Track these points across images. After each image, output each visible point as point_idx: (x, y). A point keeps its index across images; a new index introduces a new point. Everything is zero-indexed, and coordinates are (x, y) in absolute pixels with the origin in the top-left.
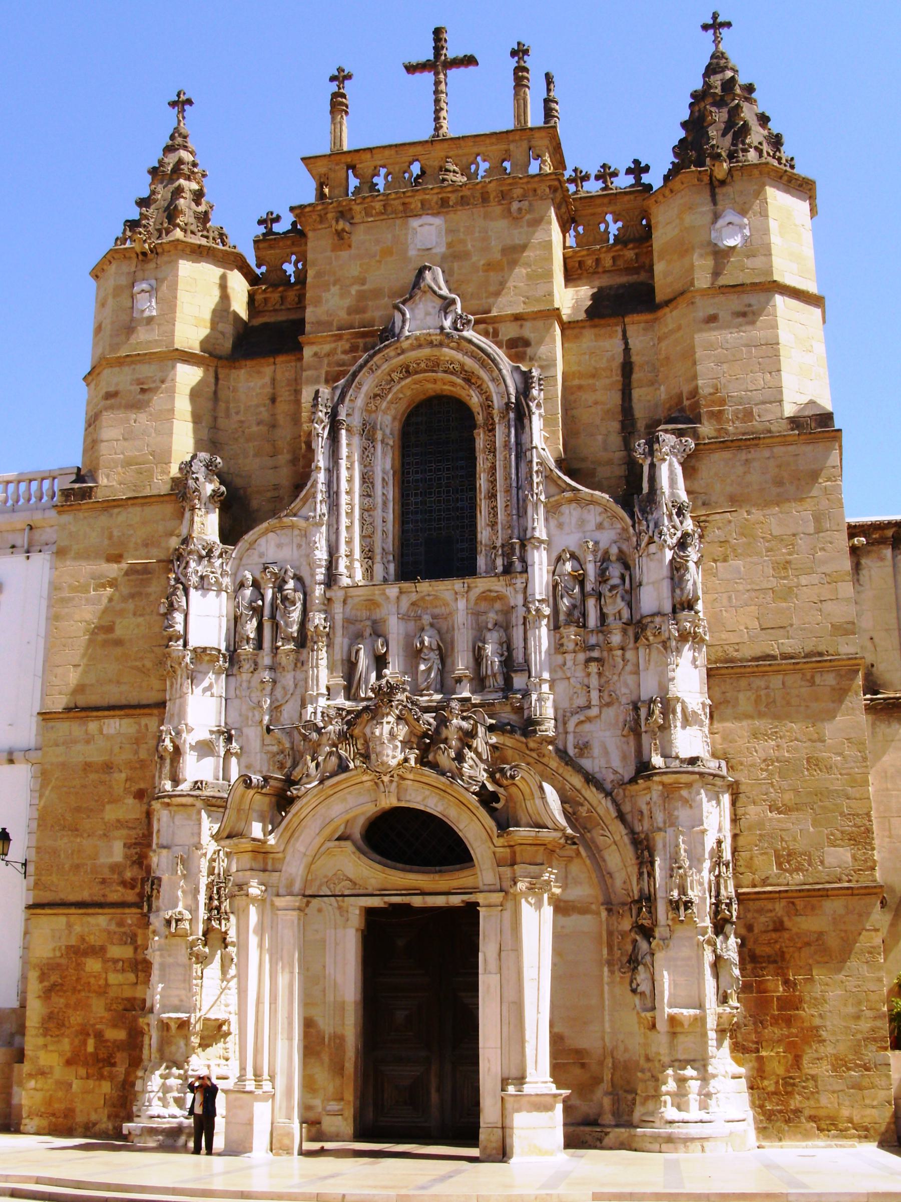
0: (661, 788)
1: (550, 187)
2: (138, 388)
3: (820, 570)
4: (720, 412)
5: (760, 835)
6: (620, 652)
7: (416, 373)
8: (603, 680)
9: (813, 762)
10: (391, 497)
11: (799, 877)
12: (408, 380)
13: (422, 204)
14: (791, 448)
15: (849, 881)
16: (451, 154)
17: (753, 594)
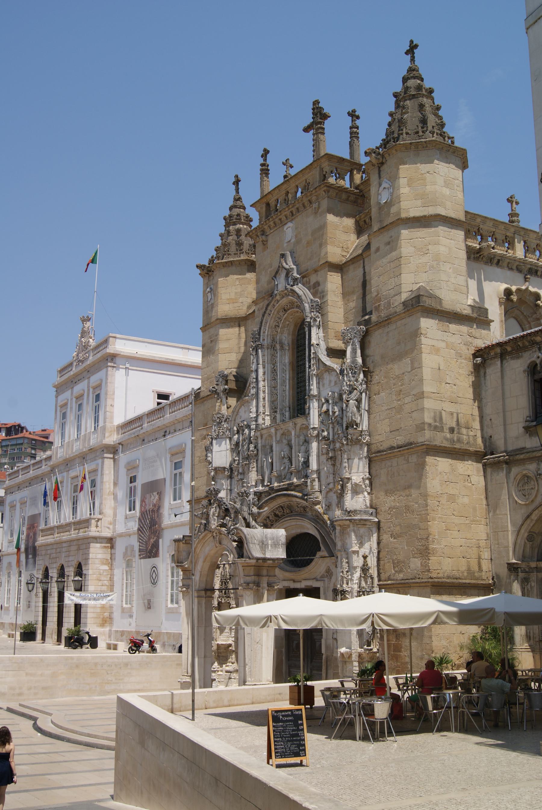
0: (339, 528)
1: (324, 191)
2: (209, 341)
3: (412, 393)
4: (379, 305)
5: (387, 551)
6: (339, 453)
7: (289, 310)
8: (336, 468)
9: (407, 508)
10: (288, 377)
11: (401, 576)
12: (286, 315)
13: (286, 217)
14: (403, 321)
15: (419, 578)
16: (297, 184)
17: (388, 411)
